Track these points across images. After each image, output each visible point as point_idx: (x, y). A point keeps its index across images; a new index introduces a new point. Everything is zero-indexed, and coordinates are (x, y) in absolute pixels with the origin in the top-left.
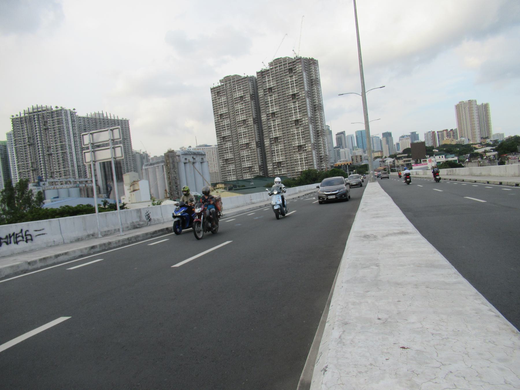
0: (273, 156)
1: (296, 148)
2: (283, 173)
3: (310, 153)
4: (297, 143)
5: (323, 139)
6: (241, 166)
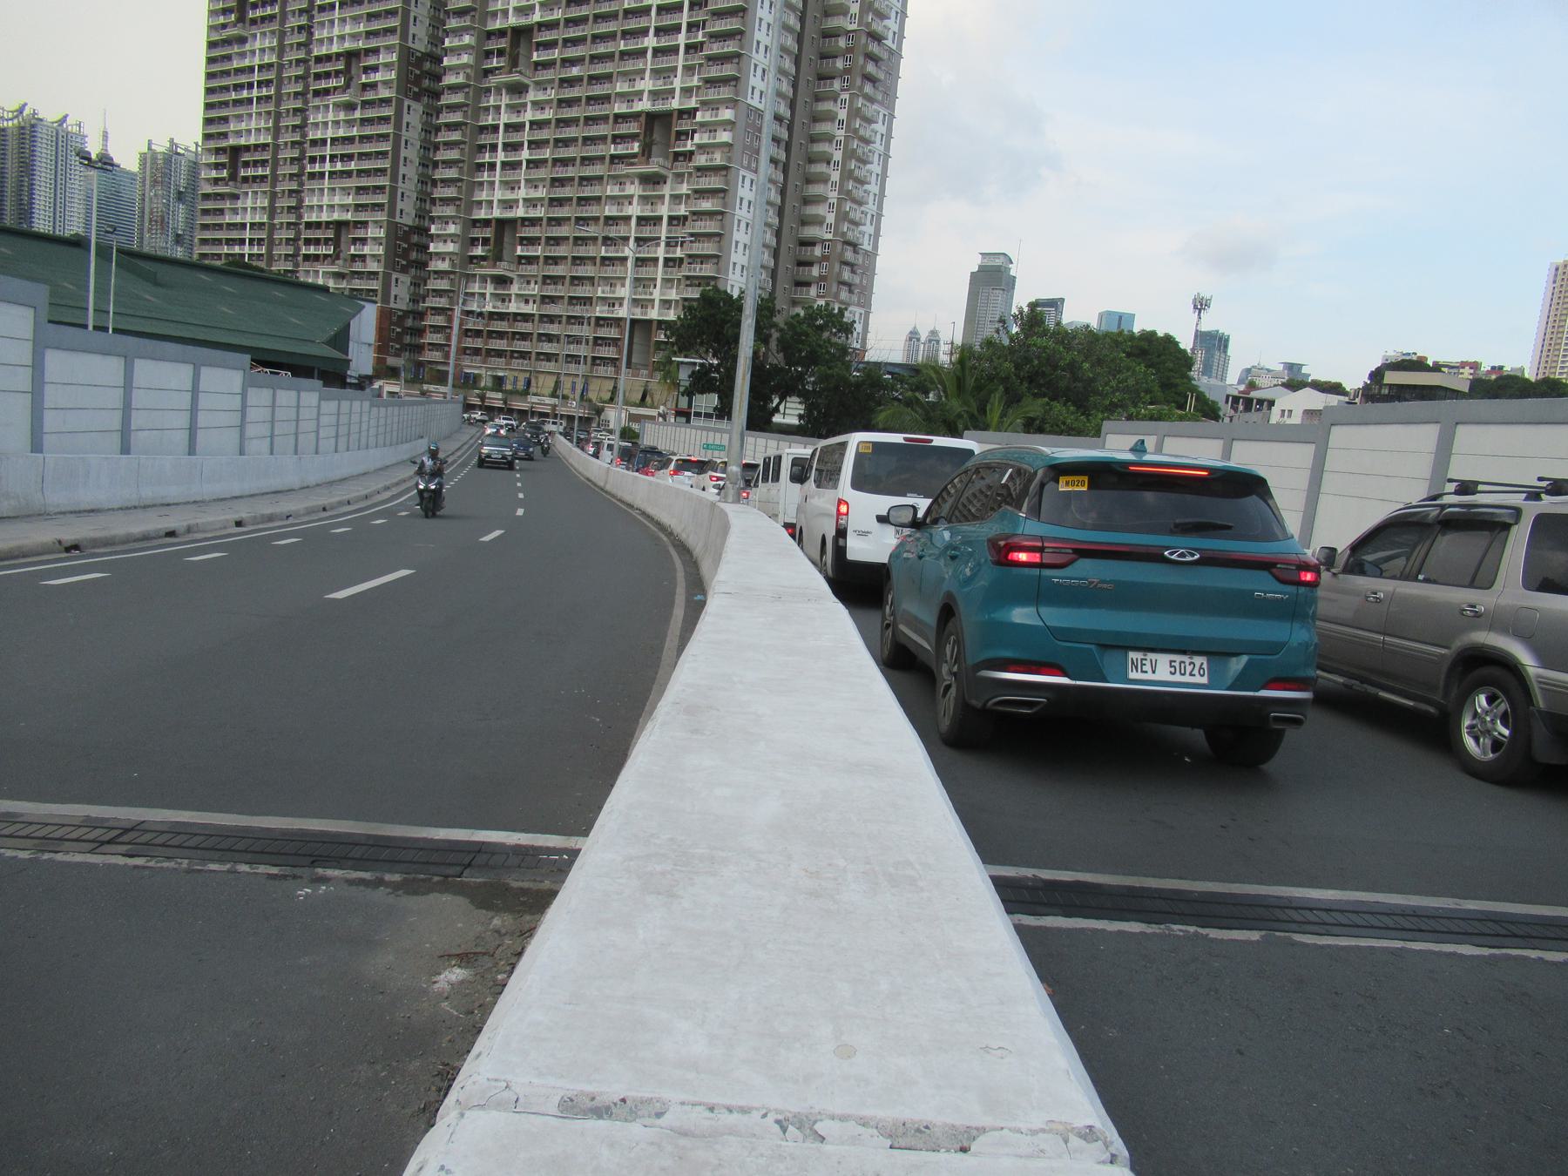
0: (480, 166)
1: (633, 128)
2: (513, 307)
3: (714, 182)
4: (642, 92)
5: (855, 113)
6: (296, 209)
